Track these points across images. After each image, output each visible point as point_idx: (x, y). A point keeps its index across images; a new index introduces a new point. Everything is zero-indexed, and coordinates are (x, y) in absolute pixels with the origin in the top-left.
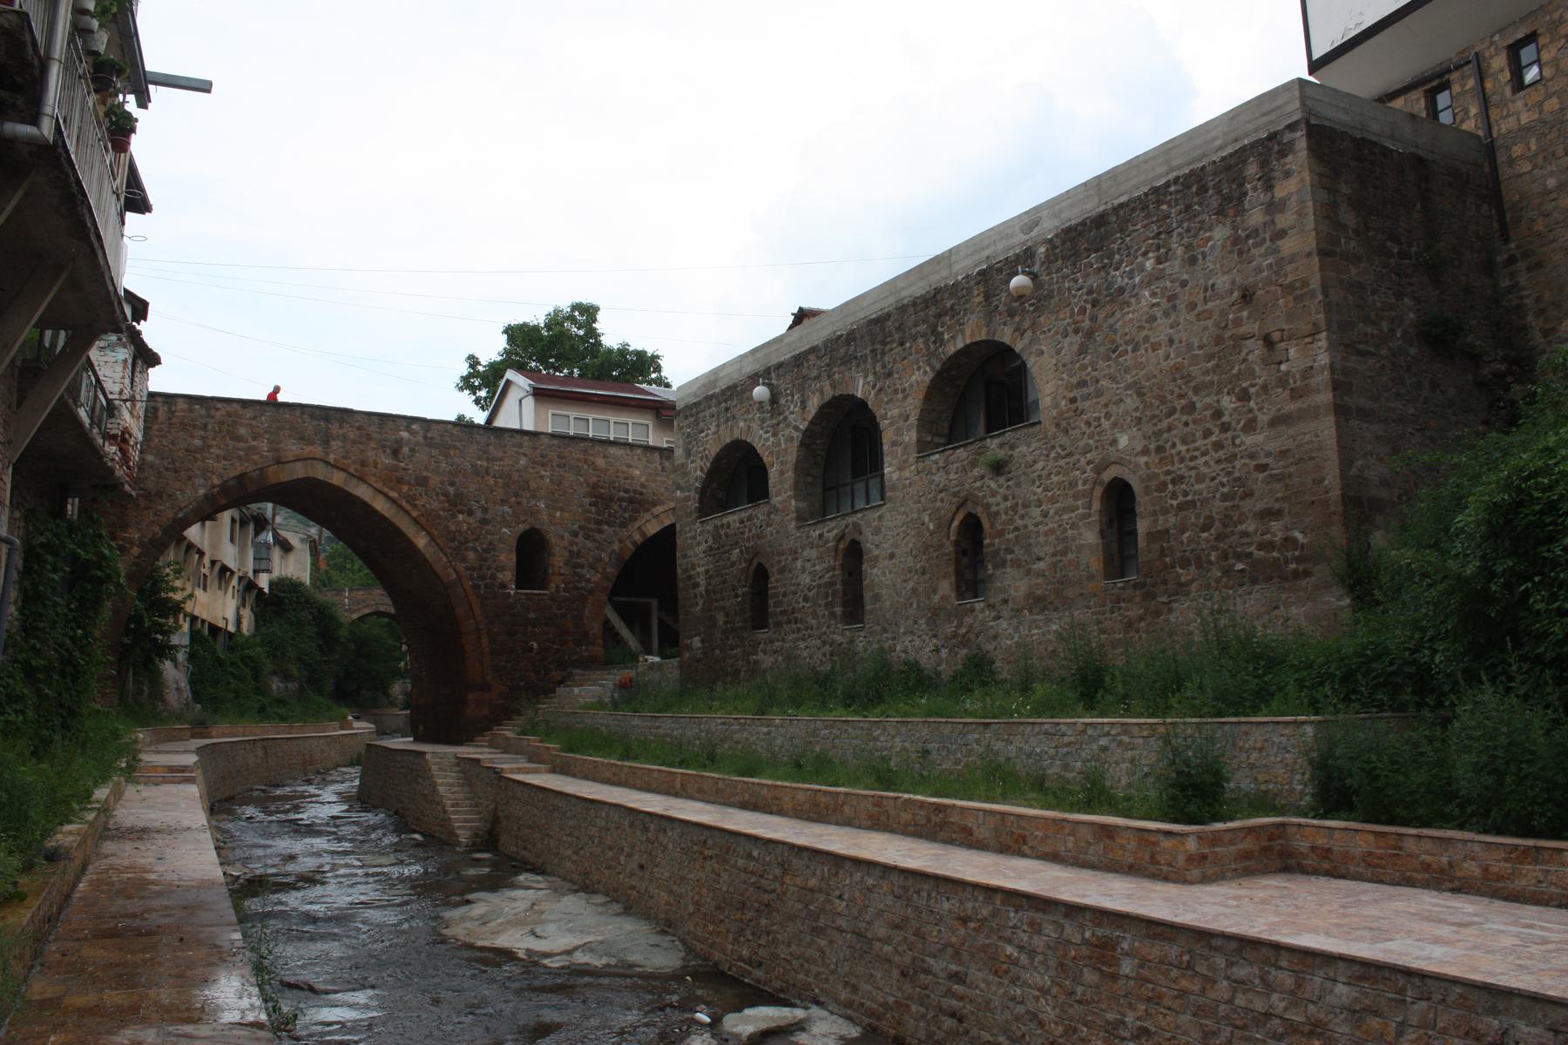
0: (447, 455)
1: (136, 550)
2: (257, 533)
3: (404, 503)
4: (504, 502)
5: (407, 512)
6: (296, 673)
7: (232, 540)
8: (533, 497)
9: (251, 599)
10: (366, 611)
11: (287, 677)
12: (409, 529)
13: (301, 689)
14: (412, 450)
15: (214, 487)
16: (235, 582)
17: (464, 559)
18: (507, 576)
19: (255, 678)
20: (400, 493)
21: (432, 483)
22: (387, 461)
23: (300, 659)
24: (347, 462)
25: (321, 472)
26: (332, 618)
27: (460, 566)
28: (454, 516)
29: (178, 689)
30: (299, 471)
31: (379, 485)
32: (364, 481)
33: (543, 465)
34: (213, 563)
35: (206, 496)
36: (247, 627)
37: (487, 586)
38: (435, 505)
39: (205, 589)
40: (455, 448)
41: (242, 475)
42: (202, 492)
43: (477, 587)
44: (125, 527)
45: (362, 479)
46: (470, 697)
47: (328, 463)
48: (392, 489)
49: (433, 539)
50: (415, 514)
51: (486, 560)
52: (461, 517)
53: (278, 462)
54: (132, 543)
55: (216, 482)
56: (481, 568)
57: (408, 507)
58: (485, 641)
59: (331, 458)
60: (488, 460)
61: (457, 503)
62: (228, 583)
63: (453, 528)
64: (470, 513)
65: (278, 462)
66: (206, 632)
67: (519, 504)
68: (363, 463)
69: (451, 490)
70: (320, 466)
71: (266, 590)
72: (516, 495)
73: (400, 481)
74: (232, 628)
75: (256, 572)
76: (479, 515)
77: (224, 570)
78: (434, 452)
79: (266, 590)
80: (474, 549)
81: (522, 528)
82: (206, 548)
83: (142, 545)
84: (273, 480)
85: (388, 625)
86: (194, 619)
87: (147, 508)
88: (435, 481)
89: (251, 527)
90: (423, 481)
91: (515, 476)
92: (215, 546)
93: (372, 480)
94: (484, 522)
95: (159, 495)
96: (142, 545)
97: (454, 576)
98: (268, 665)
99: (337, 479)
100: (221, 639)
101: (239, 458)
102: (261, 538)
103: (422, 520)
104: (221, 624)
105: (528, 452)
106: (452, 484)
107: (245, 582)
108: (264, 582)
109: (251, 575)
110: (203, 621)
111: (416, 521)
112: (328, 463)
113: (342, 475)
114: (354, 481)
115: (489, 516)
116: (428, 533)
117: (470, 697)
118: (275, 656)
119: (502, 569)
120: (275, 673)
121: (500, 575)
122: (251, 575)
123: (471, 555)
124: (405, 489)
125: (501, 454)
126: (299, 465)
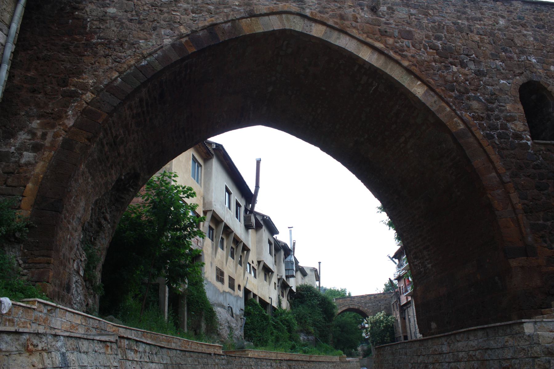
0: (426, 15)
1: (89, 96)
2: (286, 258)
3: (392, 53)
4: (495, 56)
5: (397, 62)
6: (313, 332)
7: (271, 253)
8: (523, 52)
9: (286, 294)
10: (344, 308)
11: (308, 333)
12: (405, 80)
13: (316, 341)
14: (389, 8)
15: (181, 36)
16: (274, 279)
17: (469, 109)
18: (519, 126)
19: (290, 331)
20: (385, 43)
21: (416, 36)
22: (367, 15)
23: (314, 325)
24: (326, 16)
25: (298, 25)
26: (329, 303)
27: (467, 116)
28: (447, 68)
29: (230, 327)
30: (275, 23)
31: (363, 37)
32: (346, 33)
33: (523, 26)
34: (259, 262)
35: (173, 45)
36: (285, 305)
37: (500, 136)
38: (425, 57)
39: (255, 276)
40: (433, 9)
41: (213, 25)
42: (167, 41)
43: (489, 137)
44: (79, 73)
45: (342, 31)
46: (514, 263)
47: (304, 17)
48: (376, 40)
49: (431, 88)
50: (406, 63)
51: (492, 110)
52: (455, 69)
53: (252, 15)
54: (85, 88)
55: (183, 30)
56: (489, 117)
57: (398, 57)
58: (514, 196)
59: (308, 12)
60: (468, 19)
61: (446, 55)
62: (270, 278)
63: (449, 78)
64: (463, 65)
65: (252, 15)
66: (258, 301)
67: (511, 58)
68: (342, 17)
69: (439, 44)
70: (297, 19)
71: (295, 291)
72: (505, 51)
73: (384, 33)
74: (275, 304)
75: (287, 277)
76: (472, 66)
77: (267, 271)
78: (413, 11)
79: (295, 291)
80: (477, 99)
81: (520, 80)
82: (250, 245)
83: (97, 91)
84: (247, 31)
85: (354, 316)
86: (247, 292)
87: (106, 56)
88: (419, 35)
89: (282, 253)
90: (408, 35)
91: (499, 34)
92: (259, 253)
93: (354, 32)
94: (479, 73)
95: (121, 43)
96: (97, 91)
97: (462, 126)
98: (296, 327)
99: (317, 31)
100: (269, 310)
101: (210, 12)
102: (288, 259)
103: (415, 69)
104: (268, 301)
105: (506, 14)
106: (438, 38)
107: (281, 281)
108: (293, 284)
109: (284, 277)
110: (255, 296)
111: (409, 71)
112: (304, 17)
113: (322, 28)
114: (335, 34)
115: (483, 68)
116: (424, 83)
117: (514, 263)
118: (301, 323)
119: (512, 119)
120: (301, 331)
121: (509, 125)
122: (284, 277)
123: (475, 105)
124: (391, 41)
125: (479, 15)
126: (274, 18)
